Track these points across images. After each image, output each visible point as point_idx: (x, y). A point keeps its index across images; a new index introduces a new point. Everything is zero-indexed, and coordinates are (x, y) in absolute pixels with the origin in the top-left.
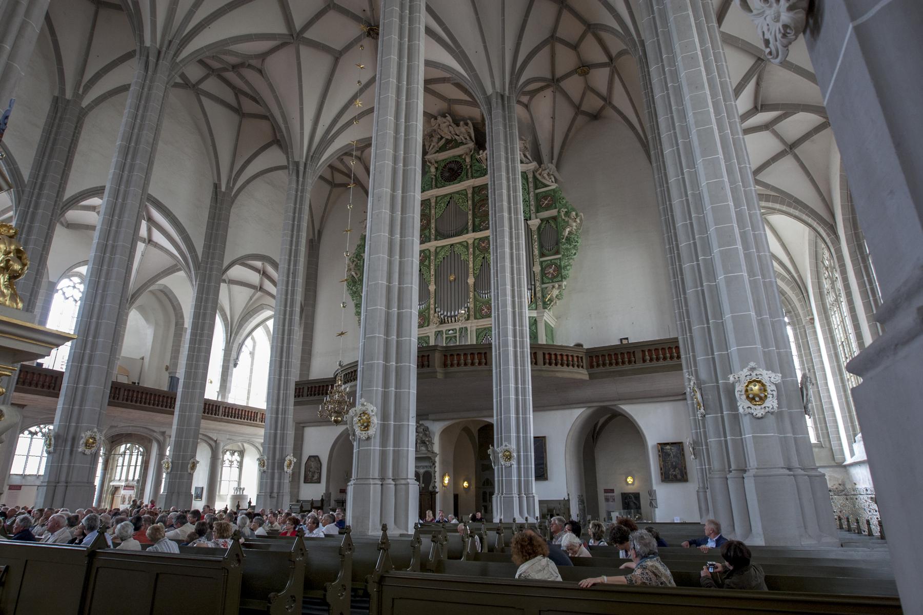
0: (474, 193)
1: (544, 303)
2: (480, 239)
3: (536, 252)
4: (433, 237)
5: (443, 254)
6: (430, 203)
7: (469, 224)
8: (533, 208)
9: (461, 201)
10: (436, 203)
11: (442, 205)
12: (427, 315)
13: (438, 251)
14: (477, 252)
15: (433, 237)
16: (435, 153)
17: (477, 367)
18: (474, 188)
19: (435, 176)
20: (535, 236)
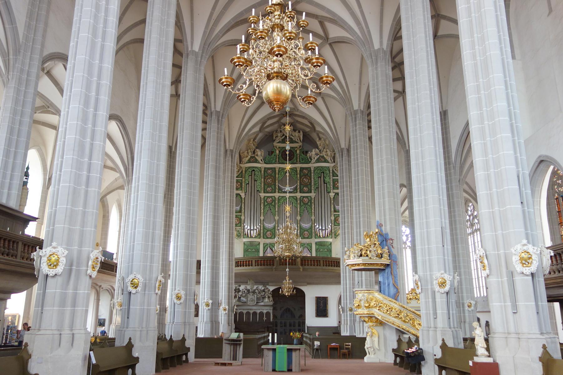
0: (300, 171)
1: (335, 235)
2: (304, 197)
3: (332, 210)
4: (277, 190)
5: (283, 200)
6: (276, 171)
7: (298, 187)
8: (332, 186)
9: (293, 173)
10: (279, 171)
11: (283, 173)
12: (273, 232)
13: (280, 198)
14: (302, 204)
15: (277, 190)
16: (278, 143)
17: (316, 267)
18: (301, 168)
19: (279, 155)
20: (332, 202)
